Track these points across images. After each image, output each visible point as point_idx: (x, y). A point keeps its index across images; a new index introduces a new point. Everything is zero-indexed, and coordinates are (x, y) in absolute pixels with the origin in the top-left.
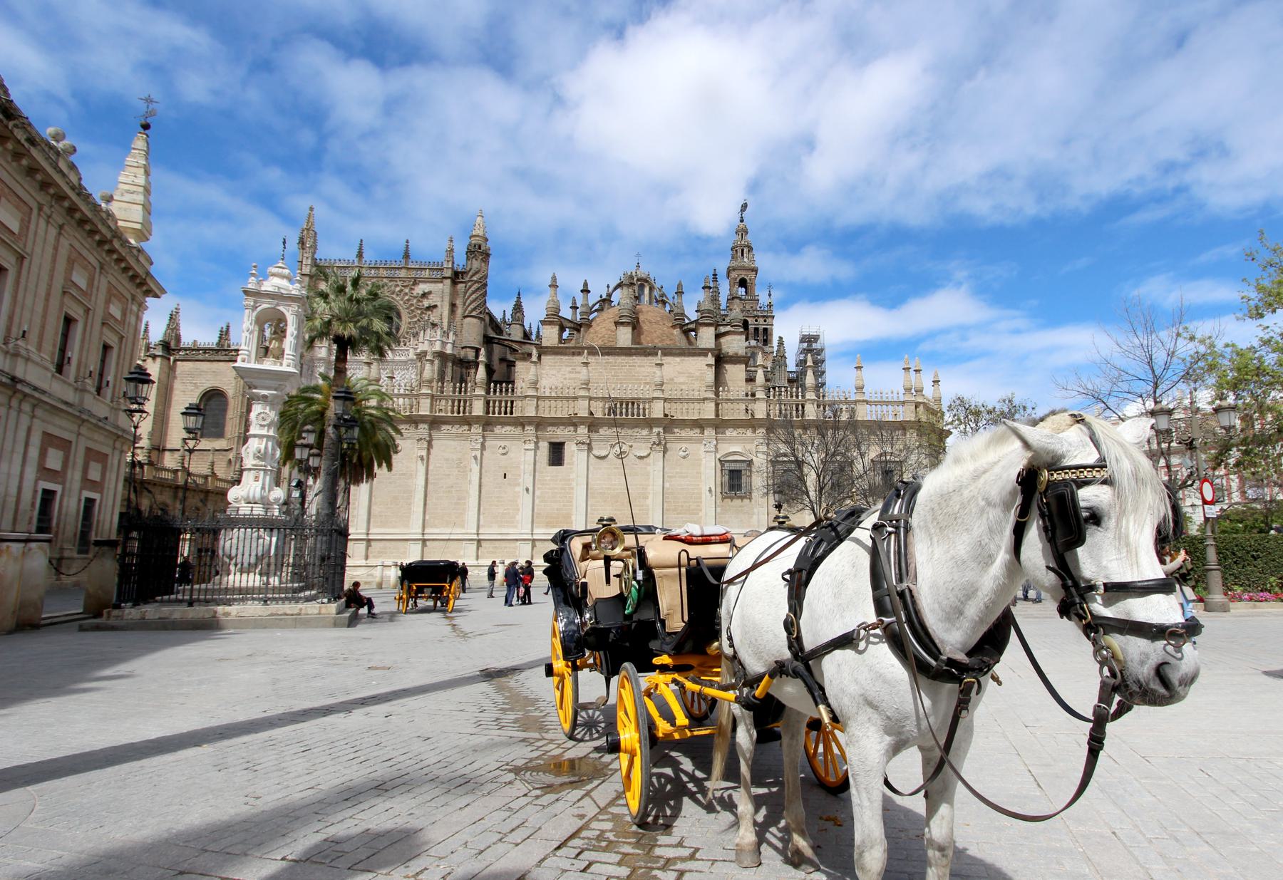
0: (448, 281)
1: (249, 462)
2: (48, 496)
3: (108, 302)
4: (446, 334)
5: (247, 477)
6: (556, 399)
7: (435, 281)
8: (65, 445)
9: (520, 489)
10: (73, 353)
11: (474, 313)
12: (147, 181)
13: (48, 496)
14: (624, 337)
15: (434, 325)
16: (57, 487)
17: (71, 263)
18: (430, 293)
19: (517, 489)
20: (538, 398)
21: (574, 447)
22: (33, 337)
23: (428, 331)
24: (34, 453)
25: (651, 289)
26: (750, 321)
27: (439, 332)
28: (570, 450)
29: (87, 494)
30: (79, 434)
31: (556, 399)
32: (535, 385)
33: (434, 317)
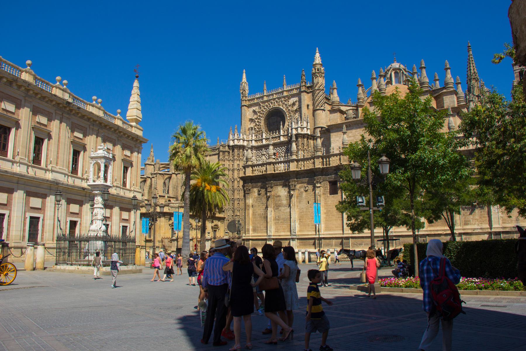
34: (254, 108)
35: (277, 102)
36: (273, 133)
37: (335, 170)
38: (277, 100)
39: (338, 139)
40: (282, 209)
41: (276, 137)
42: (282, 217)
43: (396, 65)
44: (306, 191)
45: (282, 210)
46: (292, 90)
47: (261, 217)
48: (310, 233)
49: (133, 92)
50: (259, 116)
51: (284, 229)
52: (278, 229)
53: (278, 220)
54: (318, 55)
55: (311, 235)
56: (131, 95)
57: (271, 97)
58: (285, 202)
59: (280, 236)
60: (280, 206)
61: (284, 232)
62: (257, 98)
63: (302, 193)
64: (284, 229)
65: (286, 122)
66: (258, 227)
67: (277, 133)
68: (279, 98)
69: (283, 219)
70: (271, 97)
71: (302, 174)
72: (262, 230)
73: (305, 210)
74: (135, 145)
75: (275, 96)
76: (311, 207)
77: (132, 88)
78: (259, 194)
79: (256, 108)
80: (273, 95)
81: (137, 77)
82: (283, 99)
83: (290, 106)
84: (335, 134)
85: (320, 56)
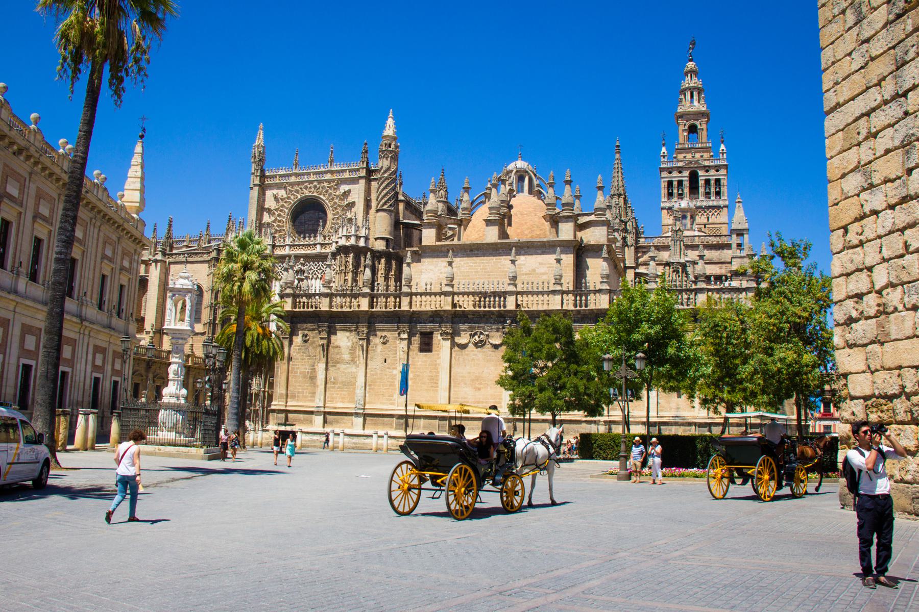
0: (362, 182)
1: (171, 376)
2: (97, 380)
3: (122, 259)
5: (171, 383)
7: (354, 181)
8: (103, 351)
10: (106, 298)
11: (385, 207)
12: (143, 173)
13: (97, 380)
14: (492, 235)
16: (100, 376)
17: (105, 243)
18: (349, 191)
21: (440, 337)
22: (89, 294)
23: (345, 229)
24: (90, 357)
25: (530, 180)
26: (701, 173)
28: (437, 337)
29: (114, 378)
30: (110, 342)
34: (275, 192)
35: (315, 187)
36: (304, 238)
37: (431, 316)
38: (315, 183)
39: (432, 267)
40: (342, 367)
41: (309, 245)
42: (340, 379)
43: (521, 164)
44: (384, 343)
45: (342, 369)
46: (345, 171)
47: (305, 377)
49: (134, 162)
50: (282, 206)
51: (343, 398)
53: (334, 383)
54: (390, 122)
56: (129, 166)
57: (306, 178)
58: (346, 357)
60: (338, 363)
61: (343, 402)
62: (281, 176)
63: (376, 345)
64: (343, 398)
65: (328, 222)
68: (320, 182)
70: (306, 178)
71: (379, 316)
72: (306, 397)
73: (379, 371)
74: (135, 250)
75: (313, 178)
77: (131, 154)
78: (306, 341)
79: (282, 193)
80: (309, 174)
81: (142, 137)
82: (326, 184)
83: (337, 196)
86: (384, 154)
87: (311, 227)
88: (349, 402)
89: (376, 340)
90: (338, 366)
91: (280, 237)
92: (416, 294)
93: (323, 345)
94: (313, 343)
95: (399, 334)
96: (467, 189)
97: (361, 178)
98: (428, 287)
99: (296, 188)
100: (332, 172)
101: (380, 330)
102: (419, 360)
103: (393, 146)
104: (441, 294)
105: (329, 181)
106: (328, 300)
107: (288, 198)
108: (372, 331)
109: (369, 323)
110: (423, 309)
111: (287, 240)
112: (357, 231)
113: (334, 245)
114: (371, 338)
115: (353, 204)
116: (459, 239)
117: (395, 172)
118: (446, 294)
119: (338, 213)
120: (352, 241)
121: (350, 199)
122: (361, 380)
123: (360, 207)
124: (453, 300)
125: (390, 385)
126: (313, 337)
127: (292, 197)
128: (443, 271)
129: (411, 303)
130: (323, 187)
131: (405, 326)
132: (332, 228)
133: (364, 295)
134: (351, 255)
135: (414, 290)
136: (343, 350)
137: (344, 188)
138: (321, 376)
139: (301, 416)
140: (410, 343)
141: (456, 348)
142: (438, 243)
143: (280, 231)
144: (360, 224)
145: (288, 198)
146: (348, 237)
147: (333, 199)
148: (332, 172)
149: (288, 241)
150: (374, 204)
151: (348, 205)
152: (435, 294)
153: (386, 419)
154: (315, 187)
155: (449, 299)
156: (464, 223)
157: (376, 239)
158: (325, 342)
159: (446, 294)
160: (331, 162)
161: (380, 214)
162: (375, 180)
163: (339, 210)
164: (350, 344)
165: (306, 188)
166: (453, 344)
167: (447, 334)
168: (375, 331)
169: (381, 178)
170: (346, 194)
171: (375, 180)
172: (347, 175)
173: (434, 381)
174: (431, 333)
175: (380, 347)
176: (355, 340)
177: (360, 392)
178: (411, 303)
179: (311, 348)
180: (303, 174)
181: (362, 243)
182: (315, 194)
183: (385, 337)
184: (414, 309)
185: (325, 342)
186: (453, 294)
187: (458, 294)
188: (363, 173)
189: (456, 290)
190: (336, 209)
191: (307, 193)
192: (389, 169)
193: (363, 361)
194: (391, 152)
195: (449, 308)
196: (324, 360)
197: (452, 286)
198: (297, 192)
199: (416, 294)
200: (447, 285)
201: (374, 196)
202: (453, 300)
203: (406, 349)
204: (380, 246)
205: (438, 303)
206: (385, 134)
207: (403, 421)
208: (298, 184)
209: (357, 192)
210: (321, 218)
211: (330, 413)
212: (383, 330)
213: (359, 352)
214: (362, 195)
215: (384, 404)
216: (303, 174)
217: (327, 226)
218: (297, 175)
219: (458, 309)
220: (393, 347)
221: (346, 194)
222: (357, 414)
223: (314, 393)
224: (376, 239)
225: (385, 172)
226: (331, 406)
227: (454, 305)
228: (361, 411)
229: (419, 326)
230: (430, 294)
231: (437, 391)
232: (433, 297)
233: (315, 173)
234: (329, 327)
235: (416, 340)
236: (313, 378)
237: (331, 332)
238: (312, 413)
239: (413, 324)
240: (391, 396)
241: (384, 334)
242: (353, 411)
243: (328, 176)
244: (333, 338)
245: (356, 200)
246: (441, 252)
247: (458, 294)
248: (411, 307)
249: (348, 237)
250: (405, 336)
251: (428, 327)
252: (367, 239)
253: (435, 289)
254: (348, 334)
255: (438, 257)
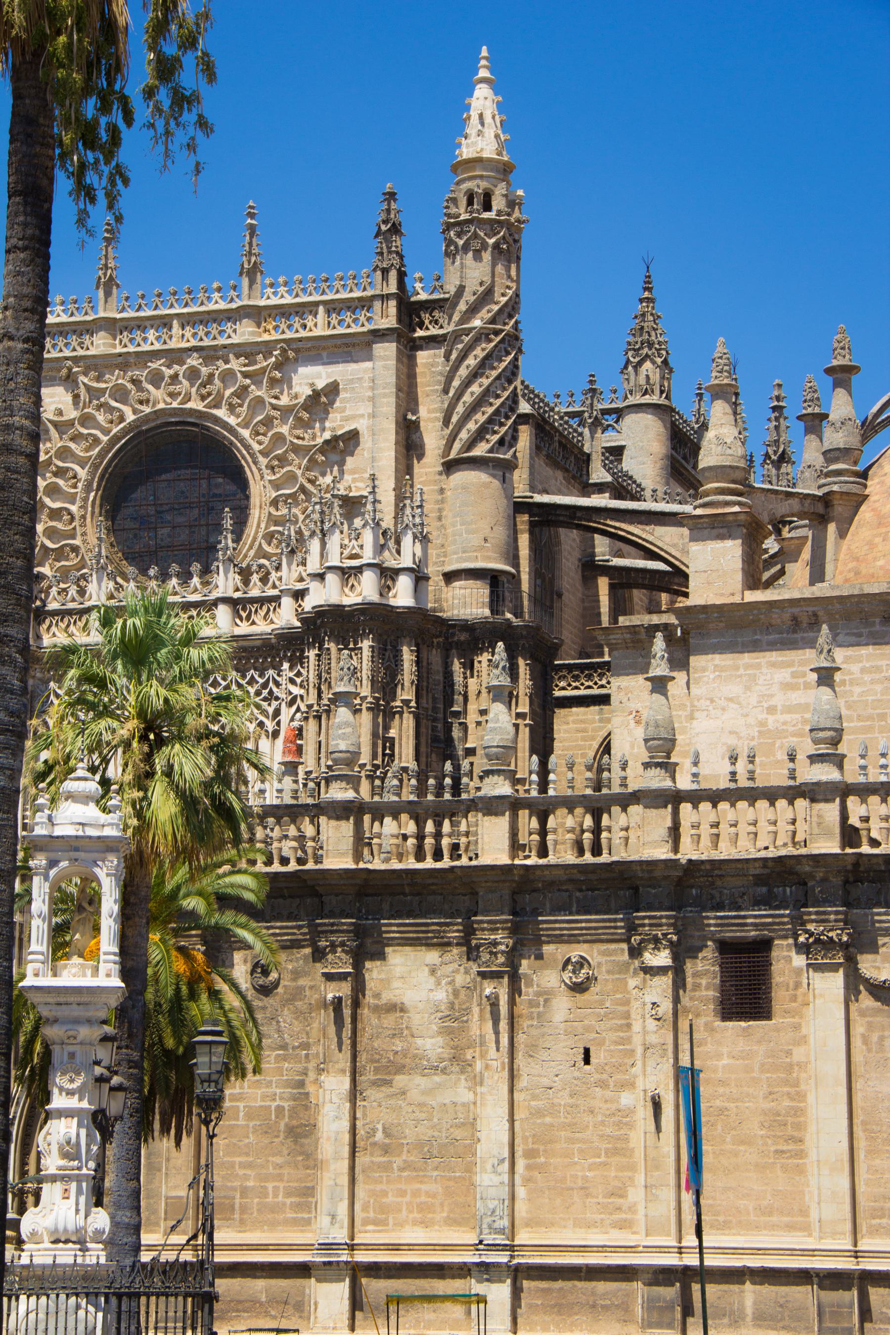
0: (386, 351)
4: (388, 539)
6: (732, 795)
9: (634, 1101)
15: (352, 506)
18: (333, 390)
19: (626, 1099)
20: (673, 799)
21: (800, 961)
23: (335, 541)
27: (368, 537)
28: (787, 962)
31: (732, 795)
32: (662, 751)
33: (353, 483)
35: (193, 374)
37: (760, 880)
38: (193, 361)
39: (734, 689)
40: (415, 1084)
42: (410, 1134)
44: (578, 988)
45: (414, 1095)
47: (267, 1130)
48: (595, 1238)
51: (421, 1208)
52: (384, 1209)
53: (386, 1150)
54: (483, 100)
55: (602, 1248)
57: (152, 341)
58: (432, 1045)
59: (395, 1247)
60: (400, 1069)
61: (425, 1224)
63: (547, 996)
64: (421, 1208)
65: (257, 515)
66: (244, 1192)
67: (196, 581)
68: (210, 354)
69: (419, 1145)
70: (152, 341)
71: (551, 885)
72: (275, 1208)
73: (563, 1099)
76: (603, 1084)
80: (164, 323)
82: (235, 364)
83: (286, 412)
84: (718, 659)
85: (501, 107)
86: (459, 236)
87: (183, 536)
88: (452, 1222)
89: (545, 977)
90: (400, 1080)
91: (64, 575)
92: (695, 798)
93: (338, 1003)
94: (297, 994)
95: (635, 952)
96: (842, 376)
97: (379, 335)
98: (741, 767)
99: (115, 378)
100: (257, 314)
101: (559, 939)
102: (728, 1049)
103: (498, 203)
104: (793, 793)
105: (247, 352)
106: (347, 828)
107: (86, 420)
108: (526, 940)
109: (509, 914)
110: (725, 851)
111: (92, 588)
112: (380, 548)
113: (287, 602)
114: (525, 966)
115: (352, 438)
116: (817, 574)
117: (512, 308)
118: (814, 793)
119: (291, 478)
120: (367, 588)
121: (336, 423)
122: (493, 1134)
123: (379, 452)
124: (844, 815)
125: (615, 1152)
126: (296, 974)
127: (101, 418)
128: (779, 700)
129: (675, 832)
130: (228, 376)
131: (658, 921)
132: (269, 537)
133: (491, 806)
134: (366, 645)
135: (684, 783)
136: (416, 1019)
137: (309, 377)
138: (332, 1123)
139: (259, 1286)
140: (679, 983)
141: (866, 1001)
142: (753, 596)
143: (60, 554)
144: (388, 522)
145: (86, 420)
146: (348, 574)
147: (268, 422)
148: (257, 314)
149: (98, 592)
150: (432, 438)
151: (331, 444)
152: (771, 795)
153: (602, 1286)
154: (193, 374)
155: (831, 811)
156: (839, 508)
157: (450, 577)
158: (344, 989)
159: (814, 793)
160: (252, 273)
161: (462, 477)
162: (433, 341)
163: (297, 466)
164: (441, 995)
165: (156, 379)
166: (855, 983)
167: (829, 945)
168: (538, 942)
169: (457, 336)
170: (321, 401)
171: (433, 341)
172: (319, 326)
173: (787, 1132)
174: (764, 946)
175: (562, 1005)
176: (461, 979)
177: (490, 1181)
178: (675, 832)
179: (286, 1016)
180: (141, 325)
181: (402, 596)
182: (195, 404)
183: (583, 962)
184: (688, 852)
185: (344, 989)
186: (844, 791)
187: (864, 791)
188: (387, 317)
189: (852, 776)
190: (283, 460)
191: (161, 398)
192: (487, 296)
193: (497, 1058)
194: (493, 226)
195: (831, 846)
196: (343, 1059)
197: (839, 761)
198: (121, 394)
199: (695, 798)
200: (814, 759)
201: (429, 413)
202: (844, 815)
203: (666, 1006)
204: (467, 603)
205: (784, 828)
206: (466, 152)
207: (671, 1292)
208: (123, 362)
209: (364, 393)
210: (225, 499)
211: (375, 1270)
212: (572, 939)
213: (479, 1025)
214: (388, 407)
215: (590, 1225)
216: (141, 325)
217: (250, 530)
218: (113, 327)
219: (866, 849)
220: (622, 1005)
221: (321, 401)
222: (486, 1271)
223: (309, 1192)
224: (450, 577)
225: (473, 310)
226: (377, 1241)
227: (850, 835)
228: (502, 1258)
229: (712, 920)
230: (752, 795)
231: (801, 1170)
232: (762, 804)
233: (187, 320)
234: (359, 932)
235: (705, 968)
236: (300, 1132)
237: (367, 948)
238: (303, 1270)
239: (689, 912)
240: (619, 1193)
241: (576, 952)
242: (470, 1258)
243: (244, 332)
244: (374, 971)
245: (362, 425)
246: (769, 628)
247: (864, 791)
248: (676, 849)
249: (348, 574)
250: (662, 958)
251: (751, 921)
252: (420, 578)
253: (774, 775)
254: (433, 956)
255: (755, 647)
